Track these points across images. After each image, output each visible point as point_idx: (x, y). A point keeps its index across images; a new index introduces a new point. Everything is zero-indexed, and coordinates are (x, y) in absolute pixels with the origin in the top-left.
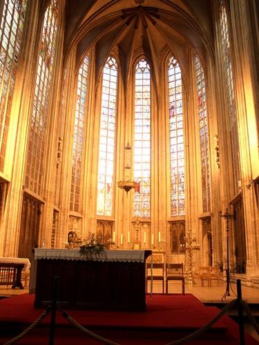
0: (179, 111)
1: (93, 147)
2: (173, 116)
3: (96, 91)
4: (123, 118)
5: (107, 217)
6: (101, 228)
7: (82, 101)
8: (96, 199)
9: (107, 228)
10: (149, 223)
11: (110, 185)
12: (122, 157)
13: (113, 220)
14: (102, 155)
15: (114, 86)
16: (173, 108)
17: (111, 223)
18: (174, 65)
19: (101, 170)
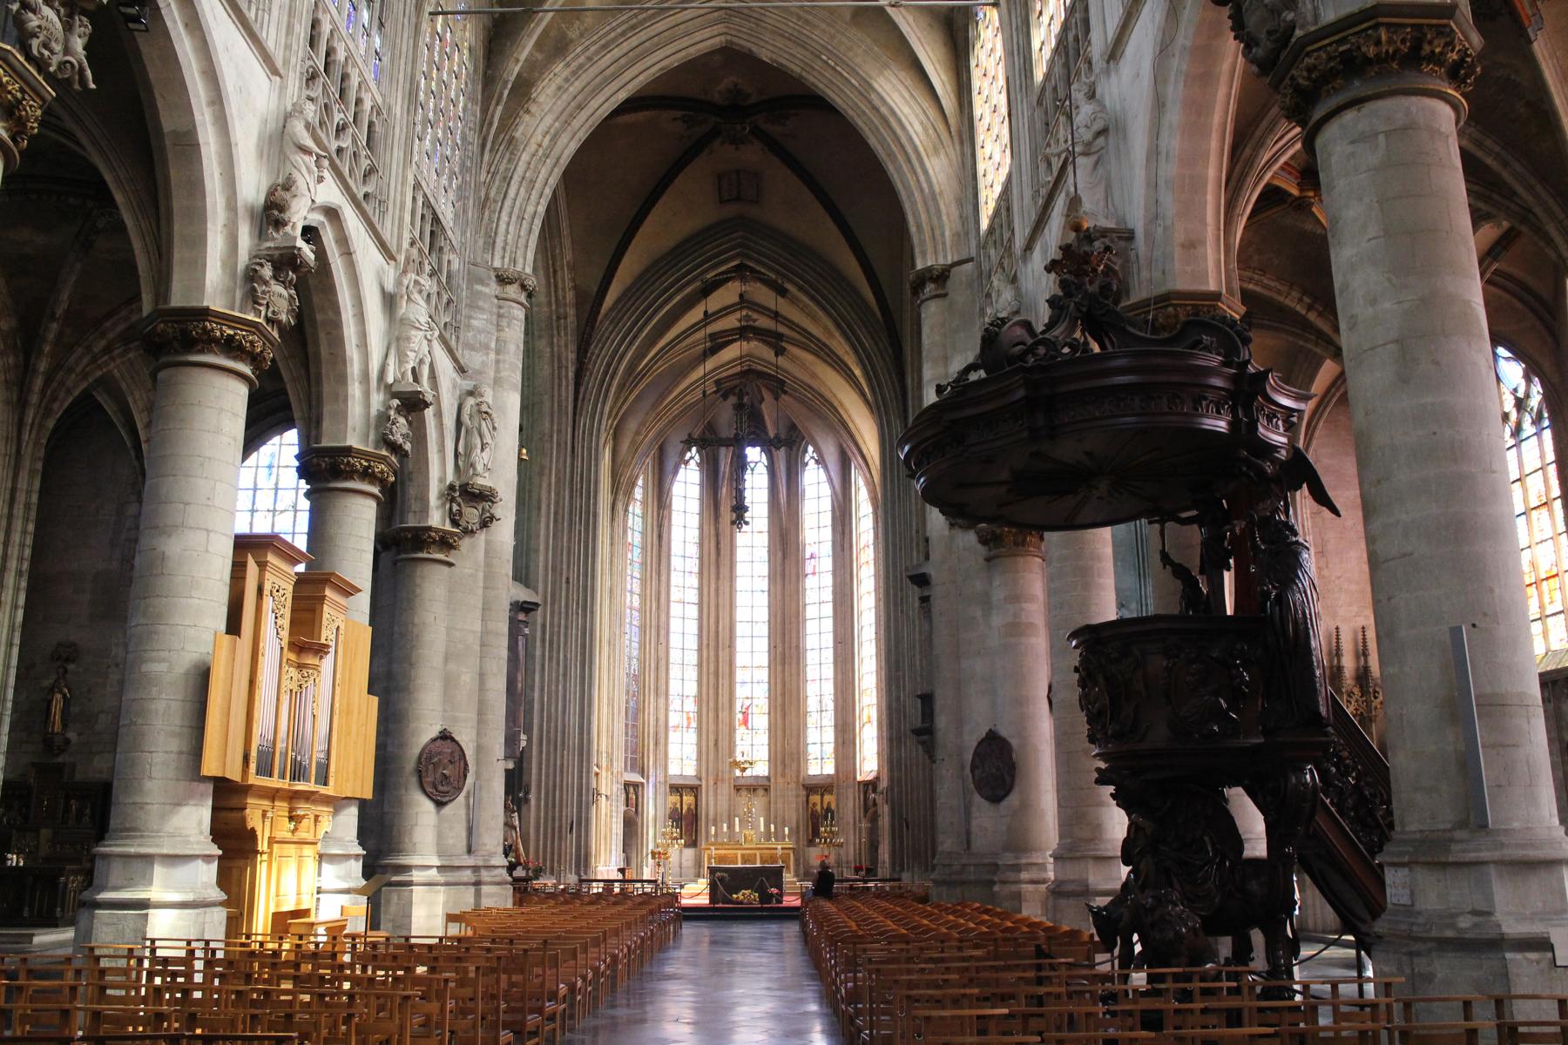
0: (826, 564)
1: (658, 643)
2: (814, 574)
3: (660, 526)
4: (713, 577)
5: (685, 777)
6: (675, 798)
7: (637, 551)
8: (666, 744)
9: (688, 799)
10: (767, 789)
11: (691, 715)
12: (712, 659)
13: (698, 783)
14: (675, 655)
15: (694, 506)
16: (812, 557)
17: (695, 790)
18: (817, 462)
19: (674, 687)
